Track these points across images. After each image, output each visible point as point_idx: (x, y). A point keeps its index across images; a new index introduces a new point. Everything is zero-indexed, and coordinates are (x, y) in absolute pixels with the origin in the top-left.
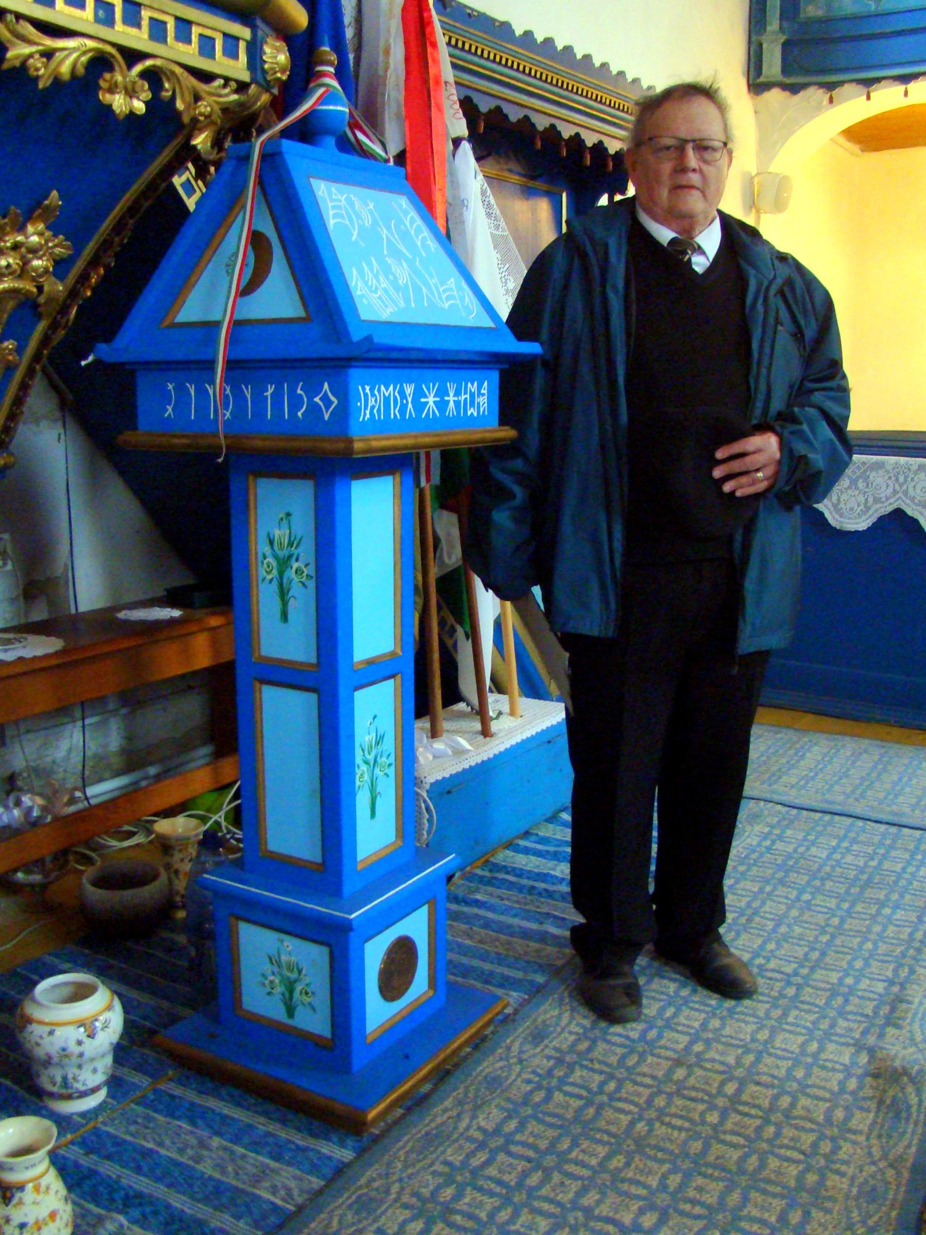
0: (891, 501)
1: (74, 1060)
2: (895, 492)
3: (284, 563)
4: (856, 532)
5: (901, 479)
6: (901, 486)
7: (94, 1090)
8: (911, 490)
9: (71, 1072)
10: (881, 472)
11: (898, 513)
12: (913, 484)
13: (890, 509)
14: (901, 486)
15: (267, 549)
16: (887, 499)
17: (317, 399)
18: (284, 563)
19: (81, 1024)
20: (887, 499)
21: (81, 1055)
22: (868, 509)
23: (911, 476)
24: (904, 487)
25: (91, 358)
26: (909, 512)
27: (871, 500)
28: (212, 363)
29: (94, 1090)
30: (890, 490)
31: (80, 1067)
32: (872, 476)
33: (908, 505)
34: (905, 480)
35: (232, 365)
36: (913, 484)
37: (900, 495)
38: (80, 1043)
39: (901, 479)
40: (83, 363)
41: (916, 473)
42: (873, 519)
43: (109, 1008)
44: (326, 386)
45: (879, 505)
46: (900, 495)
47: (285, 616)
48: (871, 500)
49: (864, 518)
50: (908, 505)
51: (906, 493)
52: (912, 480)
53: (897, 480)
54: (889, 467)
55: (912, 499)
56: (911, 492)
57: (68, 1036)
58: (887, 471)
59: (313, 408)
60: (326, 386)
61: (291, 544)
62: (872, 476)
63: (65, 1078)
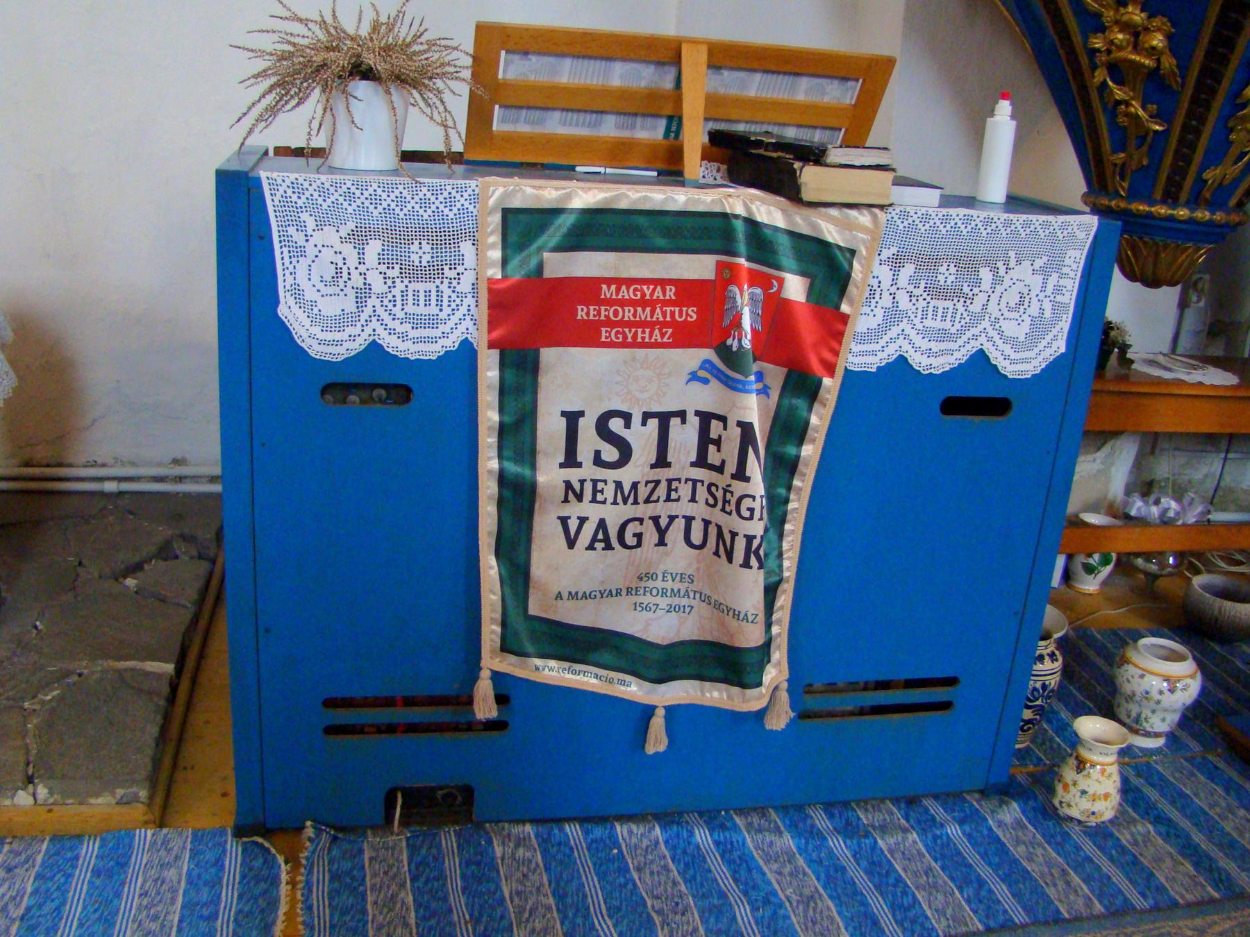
1: (1152, 704)
7: (1157, 735)
9: (1146, 712)
19: (1167, 679)
21: (1158, 702)
29: (1157, 735)
31: (1153, 712)
38: (1161, 692)
43: (1192, 676)
57: (1155, 684)
63: (1139, 715)
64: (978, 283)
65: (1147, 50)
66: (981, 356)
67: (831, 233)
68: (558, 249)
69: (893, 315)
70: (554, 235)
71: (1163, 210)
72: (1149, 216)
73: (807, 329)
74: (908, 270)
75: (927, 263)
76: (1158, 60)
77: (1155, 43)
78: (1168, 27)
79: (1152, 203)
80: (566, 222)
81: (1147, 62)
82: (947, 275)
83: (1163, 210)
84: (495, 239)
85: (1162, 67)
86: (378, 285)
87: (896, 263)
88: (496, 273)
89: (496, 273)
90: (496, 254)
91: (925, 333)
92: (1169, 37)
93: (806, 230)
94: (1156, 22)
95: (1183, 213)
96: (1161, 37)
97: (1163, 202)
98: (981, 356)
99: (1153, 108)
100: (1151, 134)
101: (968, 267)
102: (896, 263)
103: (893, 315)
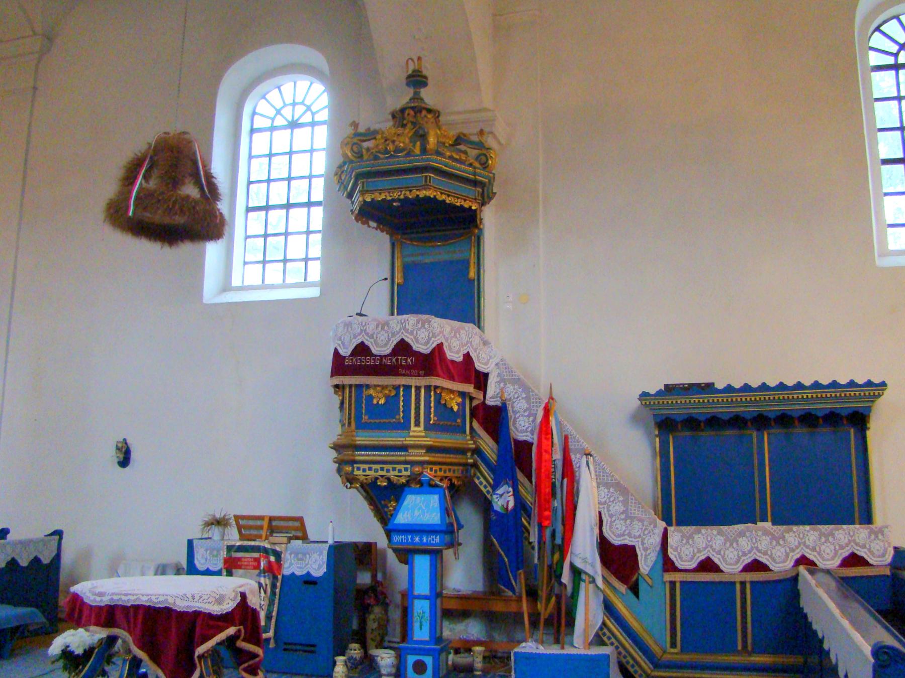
64: (306, 558)
66: (308, 573)
67: (278, 549)
68: (235, 552)
69: (291, 564)
70: (233, 550)
73: (275, 567)
74: (293, 555)
75: (297, 554)
80: (236, 547)
82: (300, 556)
84: (226, 550)
86: (208, 558)
87: (290, 554)
88: (225, 556)
89: (225, 556)
90: (225, 553)
91: (298, 567)
93: (273, 548)
98: (308, 573)
101: (304, 554)
102: (290, 554)
103: (291, 564)
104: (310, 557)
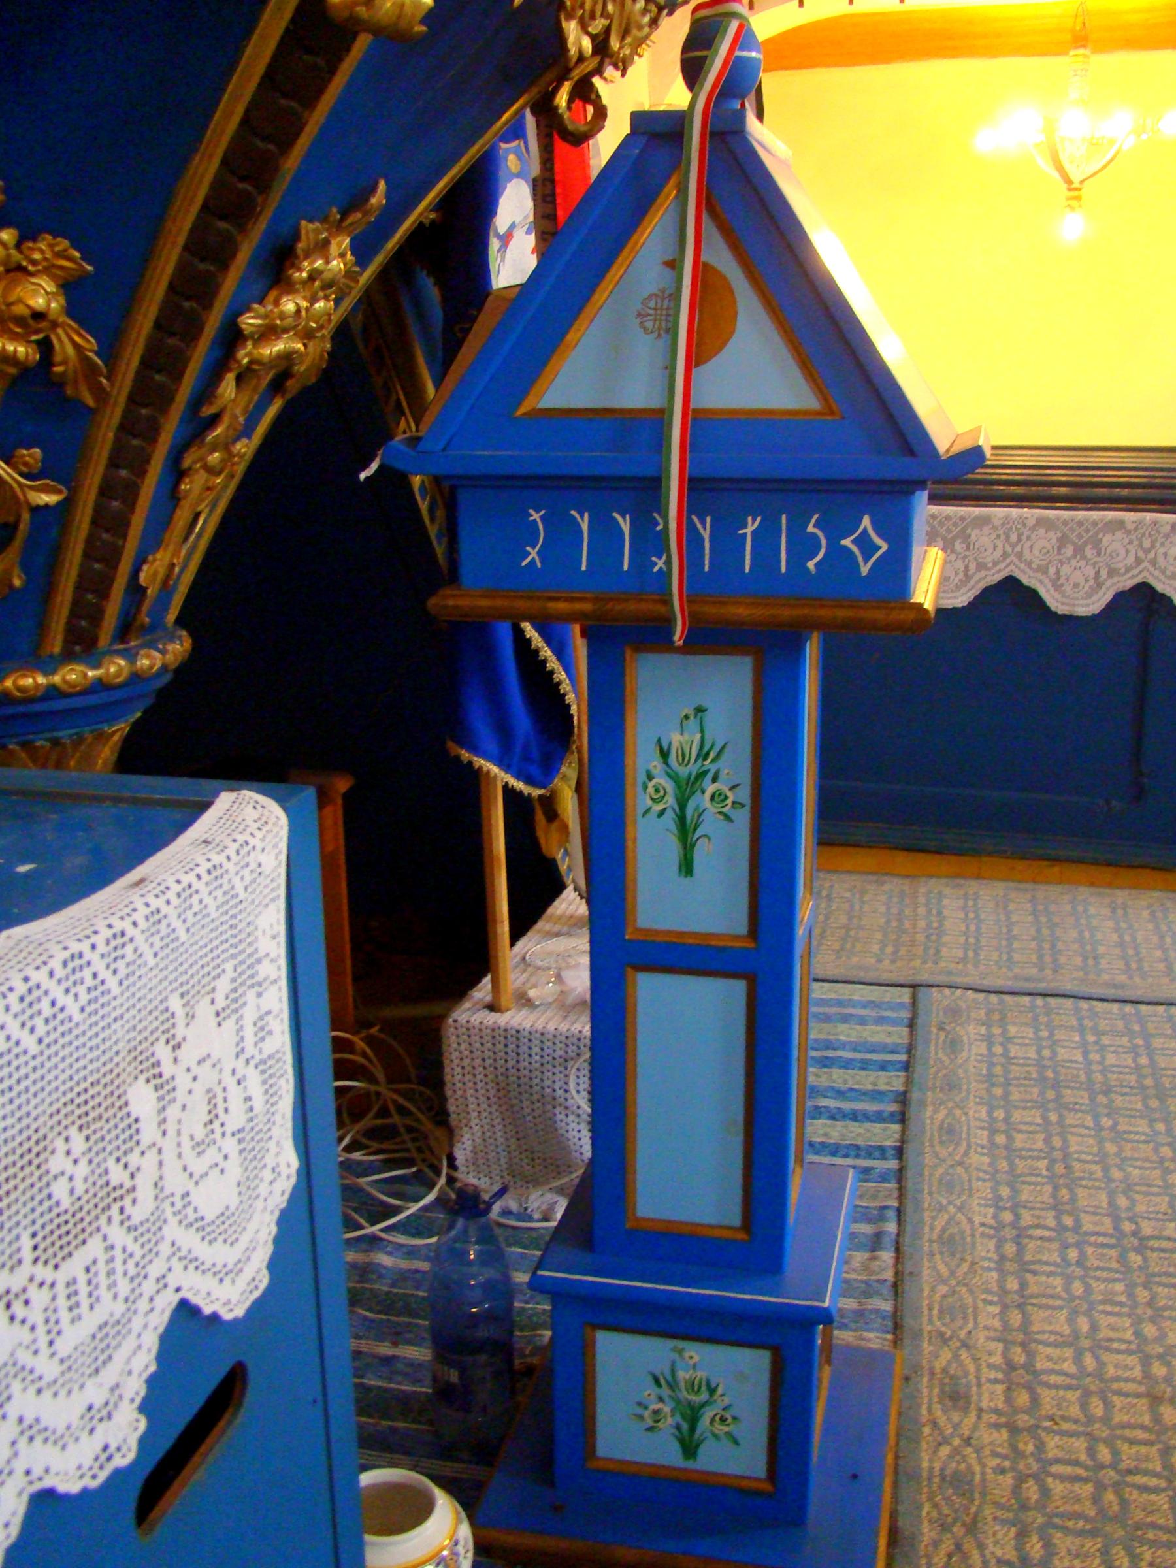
0: (1002, 566)
2: (1005, 555)
3: (687, 788)
4: (954, 609)
5: (1014, 538)
6: (1013, 546)
8: (1026, 552)
10: (986, 530)
11: (1010, 583)
12: (1029, 543)
13: (998, 578)
14: (1013, 546)
15: (656, 765)
16: (995, 564)
17: (847, 542)
18: (687, 788)
20: (995, 564)
22: (968, 577)
23: (1026, 533)
24: (1018, 549)
25: (374, 466)
26: (1025, 581)
27: (972, 567)
28: (654, 485)
30: (999, 552)
32: (974, 534)
33: (1023, 571)
34: (1019, 540)
35: (694, 486)
36: (1029, 543)
37: (1013, 558)
39: (1014, 538)
40: (363, 476)
41: (1033, 529)
42: (976, 591)
44: (866, 521)
45: (983, 573)
46: (1013, 558)
47: (687, 867)
48: (972, 567)
49: (964, 590)
50: (1023, 571)
51: (1020, 555)
52: (1028, 538)
53: (1008, 538)
54: (997, 522)
55: (1029, 564)
56: (1027, 555)
58: (995, 528)
59: (838, 554)
60: (866, 521)
61: (703, 755)
62: (974, 534)
65: (20, 320)
71: (73, 675)
72: (52, 693)
76: (45, 347)
77: (39, 302)
78: (73, 260)
79: (49, 665)
81: (21, 349)
83: (73, 675)
85: (58, 358)
92: (70, 287)
94: (43, 248)
95: (116, 668)
96: (48, 285)
97: (68, 656)
99: (33, 455)
100: (26, 516)
104: (162, 1085)
